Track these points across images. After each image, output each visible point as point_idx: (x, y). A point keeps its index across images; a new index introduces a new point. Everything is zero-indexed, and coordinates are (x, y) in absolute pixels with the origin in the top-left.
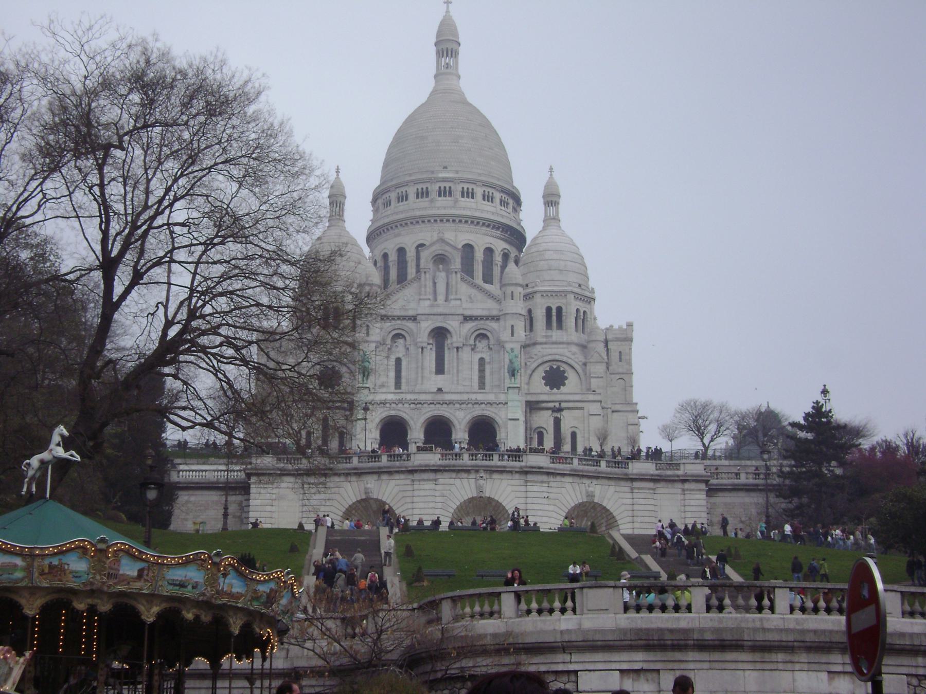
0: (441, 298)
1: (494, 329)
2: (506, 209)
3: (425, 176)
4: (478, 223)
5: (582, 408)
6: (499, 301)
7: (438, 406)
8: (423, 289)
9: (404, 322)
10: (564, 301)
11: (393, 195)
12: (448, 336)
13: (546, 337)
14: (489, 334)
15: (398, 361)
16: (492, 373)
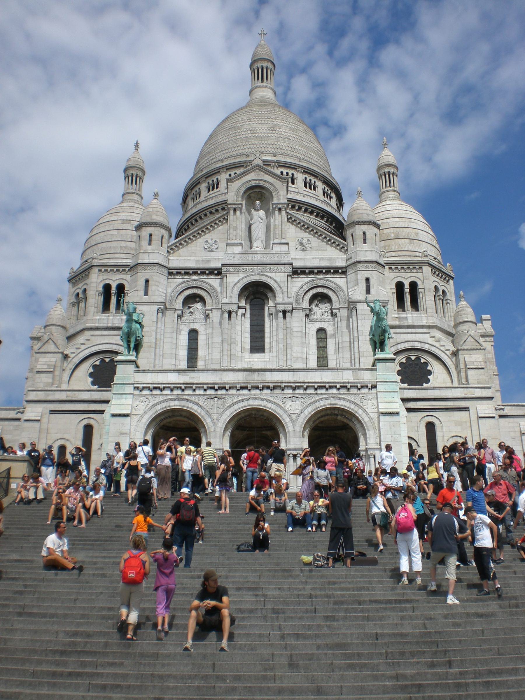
0: (258, 245)
1: (340, 287)
2: (329, 201)
3: (239, 160)
4: (300, 209)
5: (466, 409)
6: (344, 249)
7: (253, 392)
8: (231, 231)
9: (202, 278)
10: (420, 275)
11: (203, 186)
12: (270, 295)
13: (399, 318)
14: (331, 294)
15: (193, 334)
16: (337, 351)
